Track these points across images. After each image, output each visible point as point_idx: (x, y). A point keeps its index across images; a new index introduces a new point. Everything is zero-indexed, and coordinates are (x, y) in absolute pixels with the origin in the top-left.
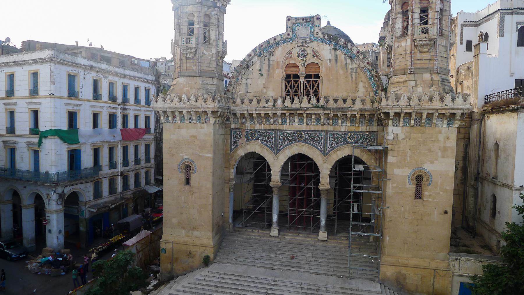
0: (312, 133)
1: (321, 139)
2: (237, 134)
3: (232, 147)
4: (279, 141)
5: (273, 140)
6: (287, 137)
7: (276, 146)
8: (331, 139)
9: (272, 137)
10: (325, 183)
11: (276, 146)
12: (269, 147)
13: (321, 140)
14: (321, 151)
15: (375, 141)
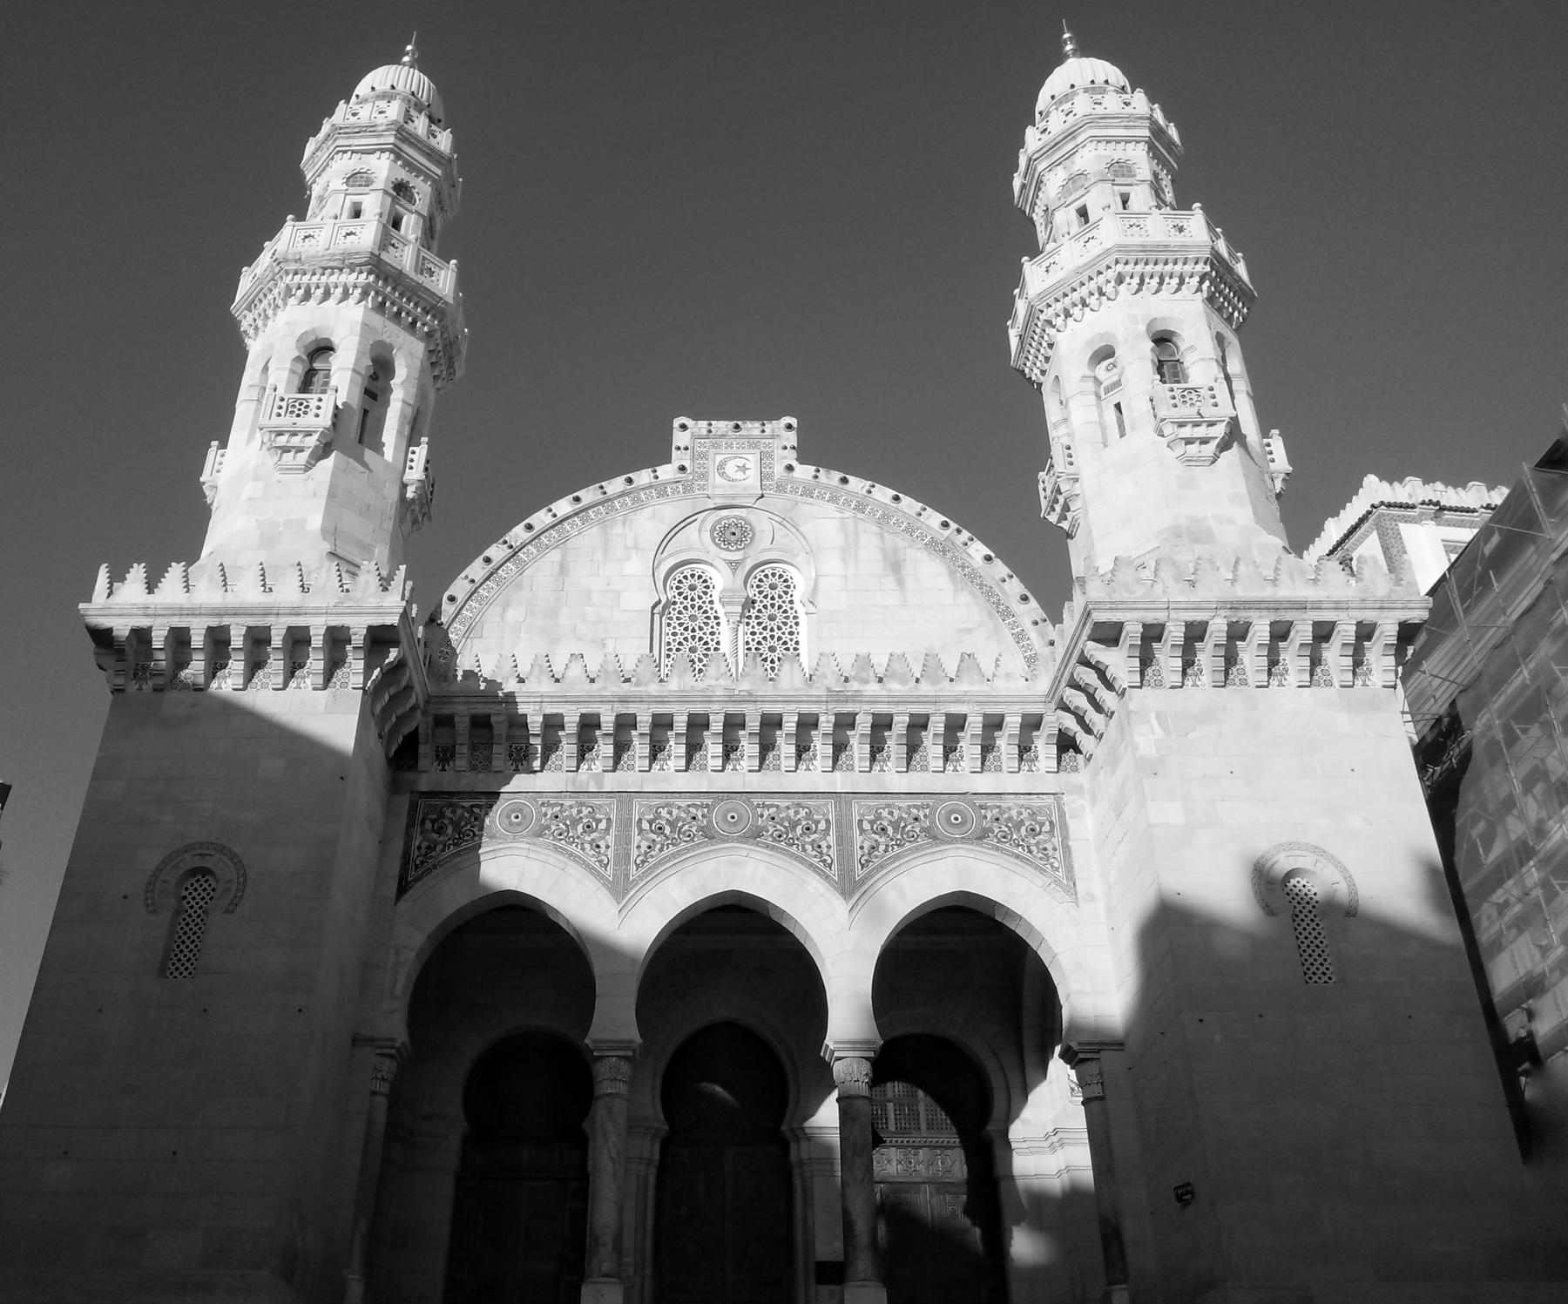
0: (783, 803)
1: (822, 826)
2: (442, 815)
3: (412, 874)
4: (636, 839)
5: (610, 839)
6: (672, 824)
7: (623, 858)
8: (866, 826)
9: (603, 825)
10: (848, 1014)
11: (623, 858)
12: (588, 867)
13: (826, 832)
14: (827, 877)
15: (1057, 831)
